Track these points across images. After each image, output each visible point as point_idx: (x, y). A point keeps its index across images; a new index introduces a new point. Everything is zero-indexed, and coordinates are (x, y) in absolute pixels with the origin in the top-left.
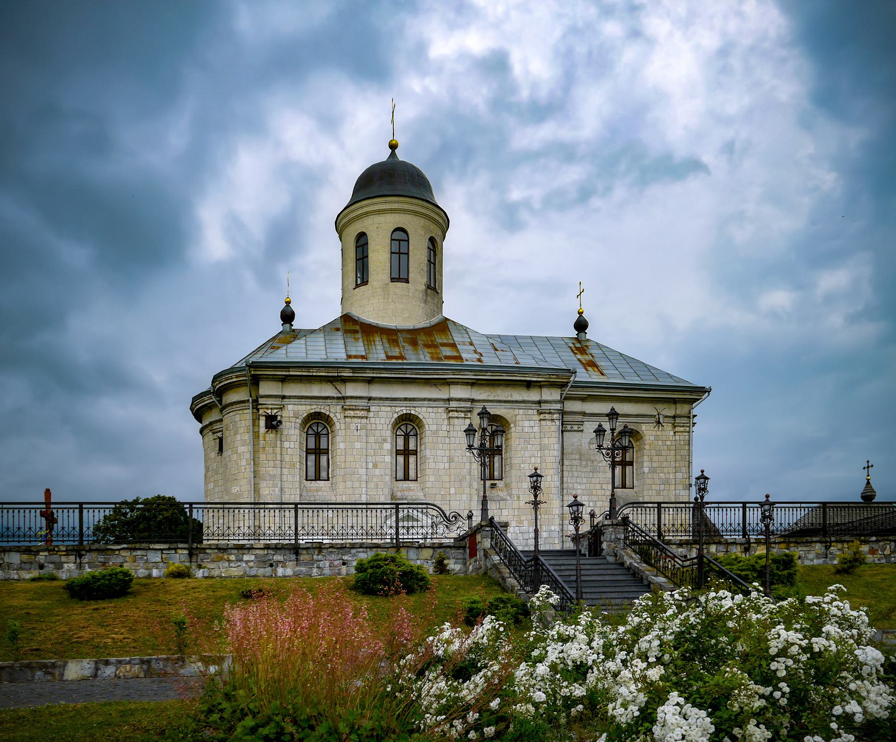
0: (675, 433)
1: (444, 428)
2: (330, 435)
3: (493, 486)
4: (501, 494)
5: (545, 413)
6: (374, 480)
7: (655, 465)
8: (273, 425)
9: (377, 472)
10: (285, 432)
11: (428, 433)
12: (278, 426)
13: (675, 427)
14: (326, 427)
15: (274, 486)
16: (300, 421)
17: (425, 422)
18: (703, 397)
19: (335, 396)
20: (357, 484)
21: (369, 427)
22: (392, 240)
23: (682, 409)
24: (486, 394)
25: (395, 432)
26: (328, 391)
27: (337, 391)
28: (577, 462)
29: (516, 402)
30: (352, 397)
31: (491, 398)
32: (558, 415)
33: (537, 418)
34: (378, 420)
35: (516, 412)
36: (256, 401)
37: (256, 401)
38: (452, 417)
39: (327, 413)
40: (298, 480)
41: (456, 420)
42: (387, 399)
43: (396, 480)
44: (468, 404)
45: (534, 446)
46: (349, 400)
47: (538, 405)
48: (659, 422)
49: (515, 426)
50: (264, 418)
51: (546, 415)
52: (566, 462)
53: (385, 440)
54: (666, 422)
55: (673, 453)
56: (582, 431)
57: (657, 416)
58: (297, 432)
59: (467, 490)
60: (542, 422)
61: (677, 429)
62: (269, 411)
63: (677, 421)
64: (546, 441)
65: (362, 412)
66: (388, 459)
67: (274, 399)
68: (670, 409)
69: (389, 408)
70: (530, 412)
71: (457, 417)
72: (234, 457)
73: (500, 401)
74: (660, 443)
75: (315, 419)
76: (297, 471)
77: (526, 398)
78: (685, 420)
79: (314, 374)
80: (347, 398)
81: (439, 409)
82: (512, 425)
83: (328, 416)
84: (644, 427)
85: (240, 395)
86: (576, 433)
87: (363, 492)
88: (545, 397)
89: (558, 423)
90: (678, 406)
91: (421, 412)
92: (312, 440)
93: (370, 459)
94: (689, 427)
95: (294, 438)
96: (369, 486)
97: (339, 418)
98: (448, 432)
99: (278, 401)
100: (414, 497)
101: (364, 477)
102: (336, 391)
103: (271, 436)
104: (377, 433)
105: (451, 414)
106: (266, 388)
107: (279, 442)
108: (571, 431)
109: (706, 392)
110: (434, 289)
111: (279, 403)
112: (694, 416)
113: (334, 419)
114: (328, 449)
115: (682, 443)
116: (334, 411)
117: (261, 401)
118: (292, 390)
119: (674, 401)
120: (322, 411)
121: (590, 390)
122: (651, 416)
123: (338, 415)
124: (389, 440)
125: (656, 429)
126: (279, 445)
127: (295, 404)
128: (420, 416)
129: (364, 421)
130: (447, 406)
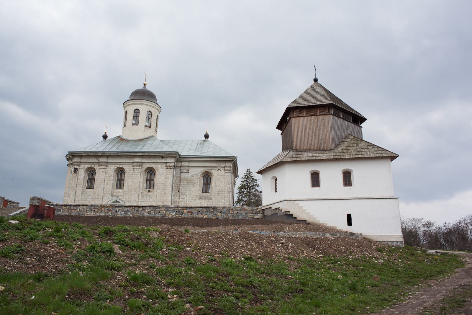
1: (132, 172)
3: (149, 191)
5: (168, 166)
7: (217, 184)
9: (108, 186)
10: (80, 173)
11: (126, 173)
15: (74, 190)
17: (125, 170)
21: (107, 171)
24: (147, 160)
26: (95, 160)
28: (186, 183)
29: (158, 163)
30: (102, 162)
31: (148, 162)
32: (173, 167)
33: (165, 168)
35: (158, 166)
38: (134, 168)
41: (136, 169)
44: (141, 164)
48: (219, 169)
49: (157, 171)
52: (182, 183)
53: (111, 176)
56: (188, 172)
58: (84, 173)
62: (75, 167)
64: (168, 176)
66: (112, 182)
68: (223, 164)
69: (114, 165)
70: (163, 166)
71: (136, 168)
73: (152, 163)
74: (219, 176)
76: (82, 186)
77: (161, 162)
80: (100, 162)
82: (156, 171)
84: (213, 171)
88: (168, 161)
89: (173, 170)
90: (226, 163)
91: (125, 167)
93: (105, 182)
95: (82, 175)
96: (104, 191)
97: (97, 168)
99: (78, 164)
104: (109, 173)
105: (134, 167)
107: (77, 176)
108: (184, 172)
111: (78, 164)
113: (96, 169)
114: (95, 179)
115: (228, 176)
116: (96, 167)
119: (225, 162)
120: (92, 166)
121: (193, 158)
122: (215, 167)
124: (113, 176)
128: (124, 168)
129: (105, 169)
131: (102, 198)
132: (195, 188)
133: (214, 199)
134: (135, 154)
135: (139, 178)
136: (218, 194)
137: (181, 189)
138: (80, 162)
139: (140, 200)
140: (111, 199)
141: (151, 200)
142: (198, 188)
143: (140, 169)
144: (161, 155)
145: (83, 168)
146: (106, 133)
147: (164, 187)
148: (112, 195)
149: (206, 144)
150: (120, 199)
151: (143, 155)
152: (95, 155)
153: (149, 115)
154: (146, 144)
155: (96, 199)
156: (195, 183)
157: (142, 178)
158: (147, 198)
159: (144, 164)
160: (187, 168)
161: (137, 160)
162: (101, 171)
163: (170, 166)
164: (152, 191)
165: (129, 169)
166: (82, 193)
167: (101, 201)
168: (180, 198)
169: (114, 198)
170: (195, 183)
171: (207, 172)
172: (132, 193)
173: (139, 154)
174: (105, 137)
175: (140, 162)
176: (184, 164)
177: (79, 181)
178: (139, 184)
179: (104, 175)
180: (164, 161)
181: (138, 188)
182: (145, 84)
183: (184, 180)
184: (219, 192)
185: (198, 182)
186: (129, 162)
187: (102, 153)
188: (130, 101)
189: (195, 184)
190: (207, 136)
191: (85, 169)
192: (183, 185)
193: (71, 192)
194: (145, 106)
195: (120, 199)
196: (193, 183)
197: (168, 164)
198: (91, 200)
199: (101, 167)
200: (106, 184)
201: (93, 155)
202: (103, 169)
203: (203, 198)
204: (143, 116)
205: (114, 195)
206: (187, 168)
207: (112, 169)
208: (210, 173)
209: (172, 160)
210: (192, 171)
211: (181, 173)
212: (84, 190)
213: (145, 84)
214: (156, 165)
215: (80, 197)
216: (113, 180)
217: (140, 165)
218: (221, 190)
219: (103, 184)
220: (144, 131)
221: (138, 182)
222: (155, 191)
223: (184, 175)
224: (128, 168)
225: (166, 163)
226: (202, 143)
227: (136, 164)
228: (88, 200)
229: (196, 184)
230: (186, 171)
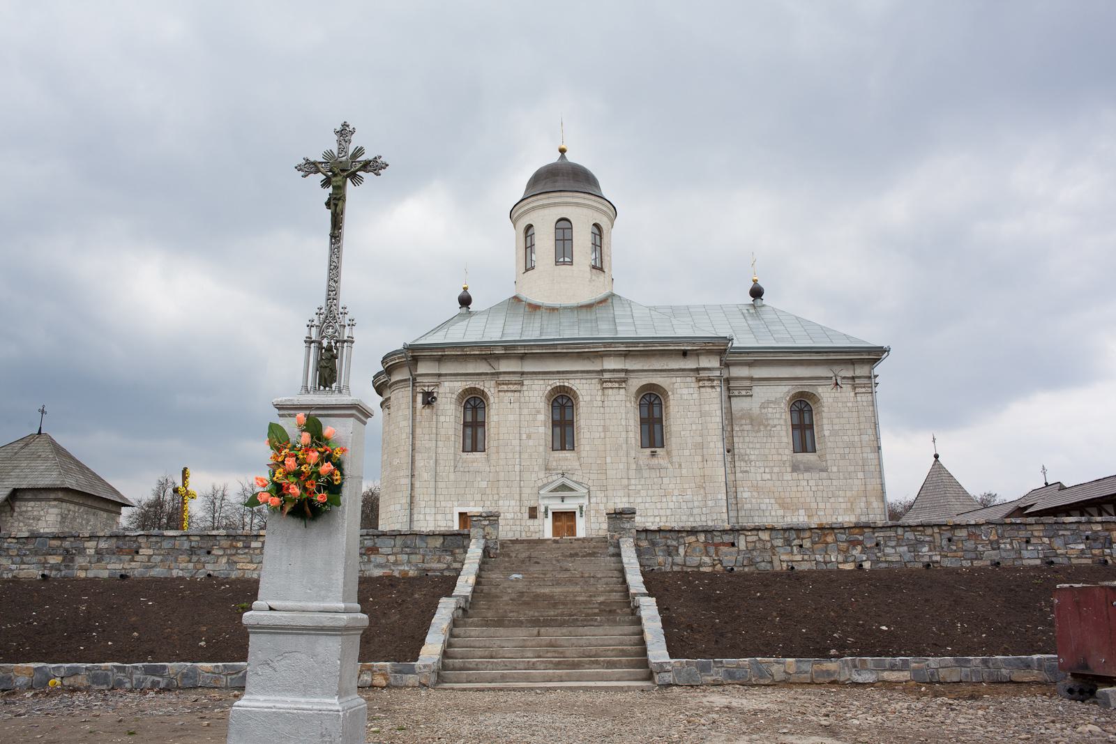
0: (856, 394)
1: (599, 398)
2: (486, 408)
3: (653, 454)
4: (661, 461)
5: (704, 380)
6: (528, 451)
7: (836, 427)
8: (429, 401)
9: (531, 443)
10: (441, 407)
11: (582, 404)
12: (433, 402)
13: (855, 388)
14: (482, 401)
15: (429, 458)
16: (456, 396)
18: (883, 356)
19: (489, 372)
20: (510, 455)
21: (522, 399)
22: (556, 229)
23: (861, 371)
24: (642, 364)
25: (550, 404)
26: (483, 368)
27: (490, 367)
28: (748, 427)
29: (673, 370)
30: (505, 373)
33: (696, 385)
34: (531, 394)
35: (674, 380)
36: (414, 380)
37: (414, 380)
38: (606, 388)
39: (482, 388)
40: (453, 452)
41: (610, 390)
42: (539, 373)
43: (553, 450)
44: (623, 375)
45: (695, 413)
46: (502, 376)
47: (696, 373)
48: (837, 384)
49: (673, 394)
50: (421, 395)
51: (705, 382)
52: (736, 428)
53: (538, 412)
54: (844, 384)
55: (855, 414)
57: (834, 378)
58: (453, 407)
59: (624, 459)
60: (701, 389)
61: (858, 390)
62: (426, 389)
63: (856, 382)
64: (707, 408)
65: (516, 386)
66: (542, 430)
67: (430, 377)
68: (847, 370)
69: (542, 382)
70: (689, 379)
72: (396, 432)
75: (472, 394)
76: (452, 443)
77: (683, 367)
78: (866, 381)
79: (468, 353)
80: (500, 373)
81: (593, 380)
82: (670, 393)
83: (483, 391)
84: (820, 390)
85: (401, 375)
86: (744, 398)
87: (517, 463)
89: (719, 389)
91: (576, 384)
92: (469, 414)
93: (523, 430)
94: (872, 387)
95: (449, 413)
96: (522, 457)
98: (603, 402)
99: (435, 380)
100: (570, 467)
101: (518, 448)
102: (490, 367)
103: (427, 411)
104: (531, 405)
106: (422, 368)
107: (434, 417)
108: (739, 396)
109: (886, 351)
110: (601, 269)
111: (436, 380)
112: (876, 376)
113: (489, 393)
115: (865, 404)
116: (488, 387)
117: (419, 379)
118: (448, 368)
119: (852, 362)
120: (477, 386)
122: (827, 378)
123: (492, 390)
124: (543, 413)
125: (834, 391)
126: (434, 420)
127: (451, 381)
128: (573, 388)
129: (517, 394)
130: (601, 377)
131: (518, 479)
132: (775, 440)
133: (835, 469)
134: (604, 347)
135: (624, 416)
136: (843, 457)
137: (736, 446)
138: (439, 375)
139: (633, 482)
140: (545, 481)
141: (666, 480)
142: (785, 440)
143: (622, 391)
144: (683, 348)
145: (449, 391)
146: (465, 289)
147: (699, 439)
148: (546, 469)
149: (768, 316)
150: (574, 479)
151: (631, 349)
152: (483, 353)
153: (595, 234)
154: (614, 317)
155: (501, 483)
156: (775, 426)
157: (631, 415)
158: (654, 474)
159: (632, 375)
160: (747, 383)
161: (610, 364)
162: (506, 400)
163: (709, 380)
164: (661, 453)
165: (589, 392)
166: (455, 467)
167: (518, 489)
168: (738, 470)
169: (555, 477)
170: (775, 426)
171: (802, 394)
172: (609, 460)
173: (617, 345)
174: (465, 301)
175: (622, 371)
176: (736, 372)
177: (442, 432)
178: (624, 434)
179: (517, 410)
180: (690, 364)
181: (624, 446)
182: (562, 151)
183: (741, 418)
184: (847, 450)
185: (782, 422)
186: (588, 372)
187: (506, 348)
188: (539, 197)
189: (775, 429)
190: (757, 293)
191: (457, 393)
192: (740, 434)
193: (422, 464)
194: (585, 211)
196: (769, 425)
197: (703, 374)
198: (484, 484)
199: (505, 387)
200: (524, 437)
201: (477, 353)
202: (513, 394)
203: (802, 467)
204: (582, 238)
205: (554, 470)
206: (747, 383)
207: (537, 393)
208: (812, 396)
209: (714, 362)
210: (762, 393)
211: (730, 397)
212: (459, 457)
213: (562, 151)
214: (668, 377)
215: (452, 477)
216: (545, 426)
217: (622, 378)
218: (851, 445)
219: (517, 436)
220: (590, 281)
221: (621, 428)
222: (674, 453)
223: (739, 404)
224: (585, 390)
225: (698, 370)
226: (752, 311)
227: (609, 376)
228: (476, 484)
229: (778, 428)
230: (744, 393)
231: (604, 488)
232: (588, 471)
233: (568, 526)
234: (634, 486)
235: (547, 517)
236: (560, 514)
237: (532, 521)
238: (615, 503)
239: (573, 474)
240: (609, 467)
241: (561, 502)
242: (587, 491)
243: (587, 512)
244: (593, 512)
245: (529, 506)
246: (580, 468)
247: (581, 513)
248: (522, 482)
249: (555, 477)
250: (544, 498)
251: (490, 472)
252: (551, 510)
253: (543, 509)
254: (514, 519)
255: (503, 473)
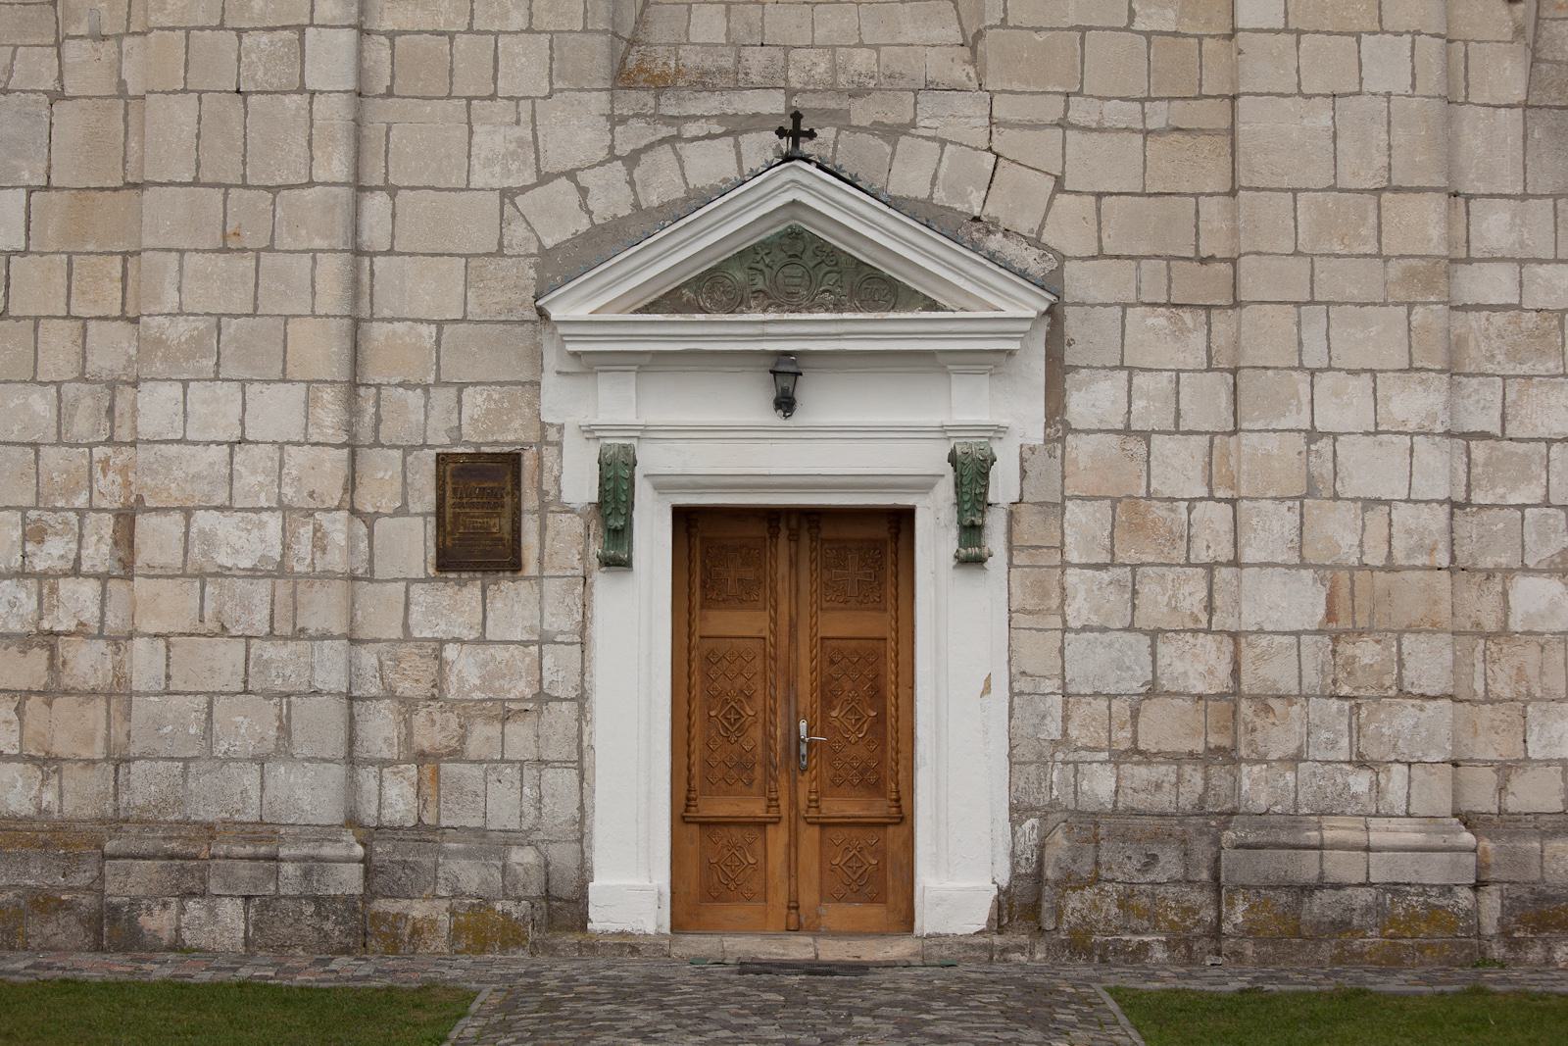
100: (862, 60)
131: (335, 165)
139: (1495, 227)
140: (610, 197)
148: (623, 78)
150: (910, 179)
167: (332, 268)
169: (709, 163)
195: (893, 203)
205: (703, 82)
231: (1209, 284)
232: (1053, 109)
233: (831, 652)
234: (1505, 274)
235: (617, 561)
236: (759, 530)
237: (472, 592)
238: (1312, 435)
239: (892, 133)
240: (1264, 67)
241: (775, 419)
242: (1031, 304)
243: (1028, 518)
244: (1084, 525)
245: (441, 439)
246: (961, 73)
247: (971, 531)
248: (376, 205)
249: (709, 163)
250: (590, 365)
251: (57, 96)
252: (663, 484)
253: (580, 484)
254: (281, 571)
255: (184, 112)
